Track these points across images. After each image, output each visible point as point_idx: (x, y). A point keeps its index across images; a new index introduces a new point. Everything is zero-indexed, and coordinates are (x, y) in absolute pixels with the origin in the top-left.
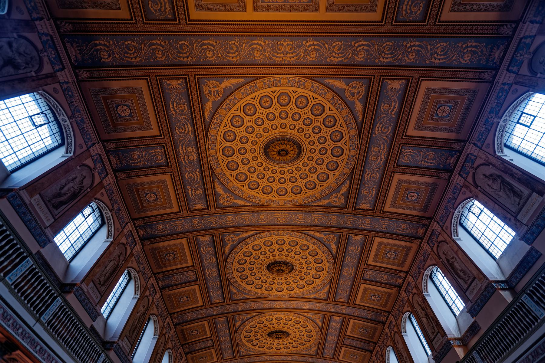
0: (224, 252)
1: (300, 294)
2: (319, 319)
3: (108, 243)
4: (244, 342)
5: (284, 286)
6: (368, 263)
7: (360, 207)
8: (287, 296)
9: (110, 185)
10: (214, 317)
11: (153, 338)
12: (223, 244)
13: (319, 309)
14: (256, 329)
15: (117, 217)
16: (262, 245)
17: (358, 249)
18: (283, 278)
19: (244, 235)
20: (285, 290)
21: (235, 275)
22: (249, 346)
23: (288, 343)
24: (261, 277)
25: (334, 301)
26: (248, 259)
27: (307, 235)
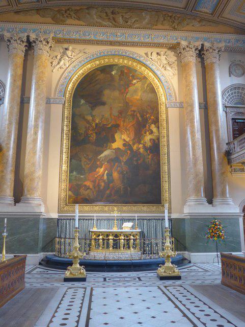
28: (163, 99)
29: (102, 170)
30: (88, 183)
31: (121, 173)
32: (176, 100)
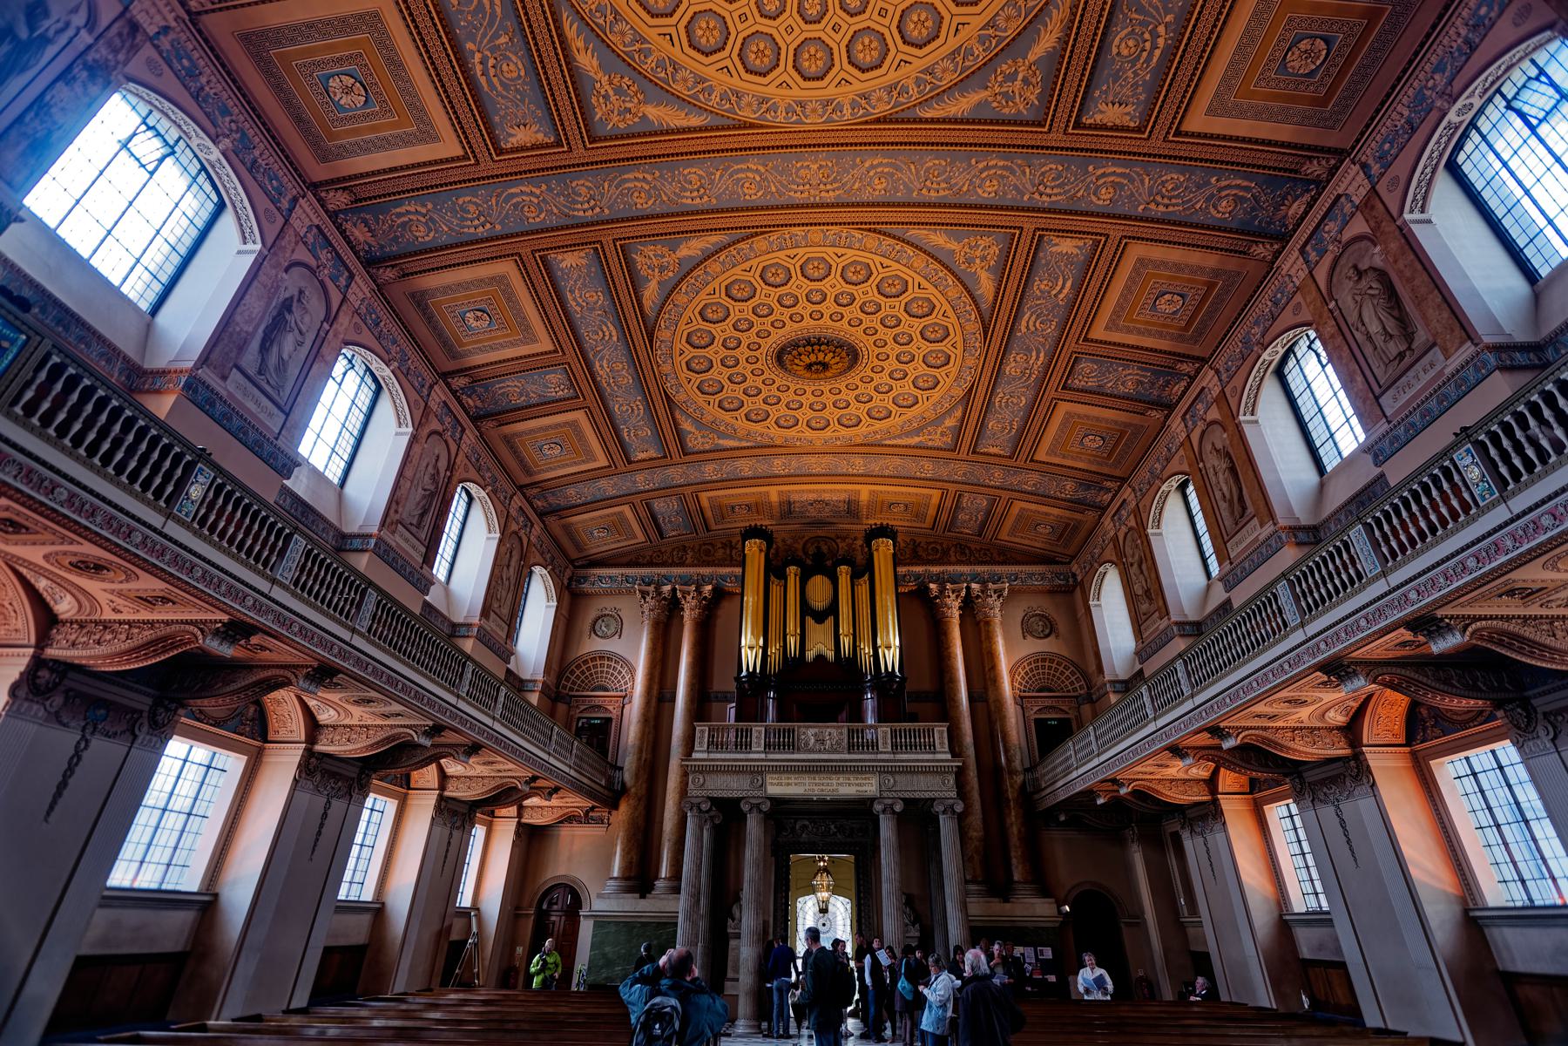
3: (250, 259)
5: (831, 414)
6: (1090, 336)
7: (1098, 117)
9: (172, 36)
10: (645, 496)
11: (488, 539)
12: (636, 283)
15: (250, 171)
16: (759, 284)
17: (1063, 287)
18: (826, 389)
19: (692, 248)
20: (834, 425)
24: (761, 386)
25: (974, 452)
26: (716, 329)
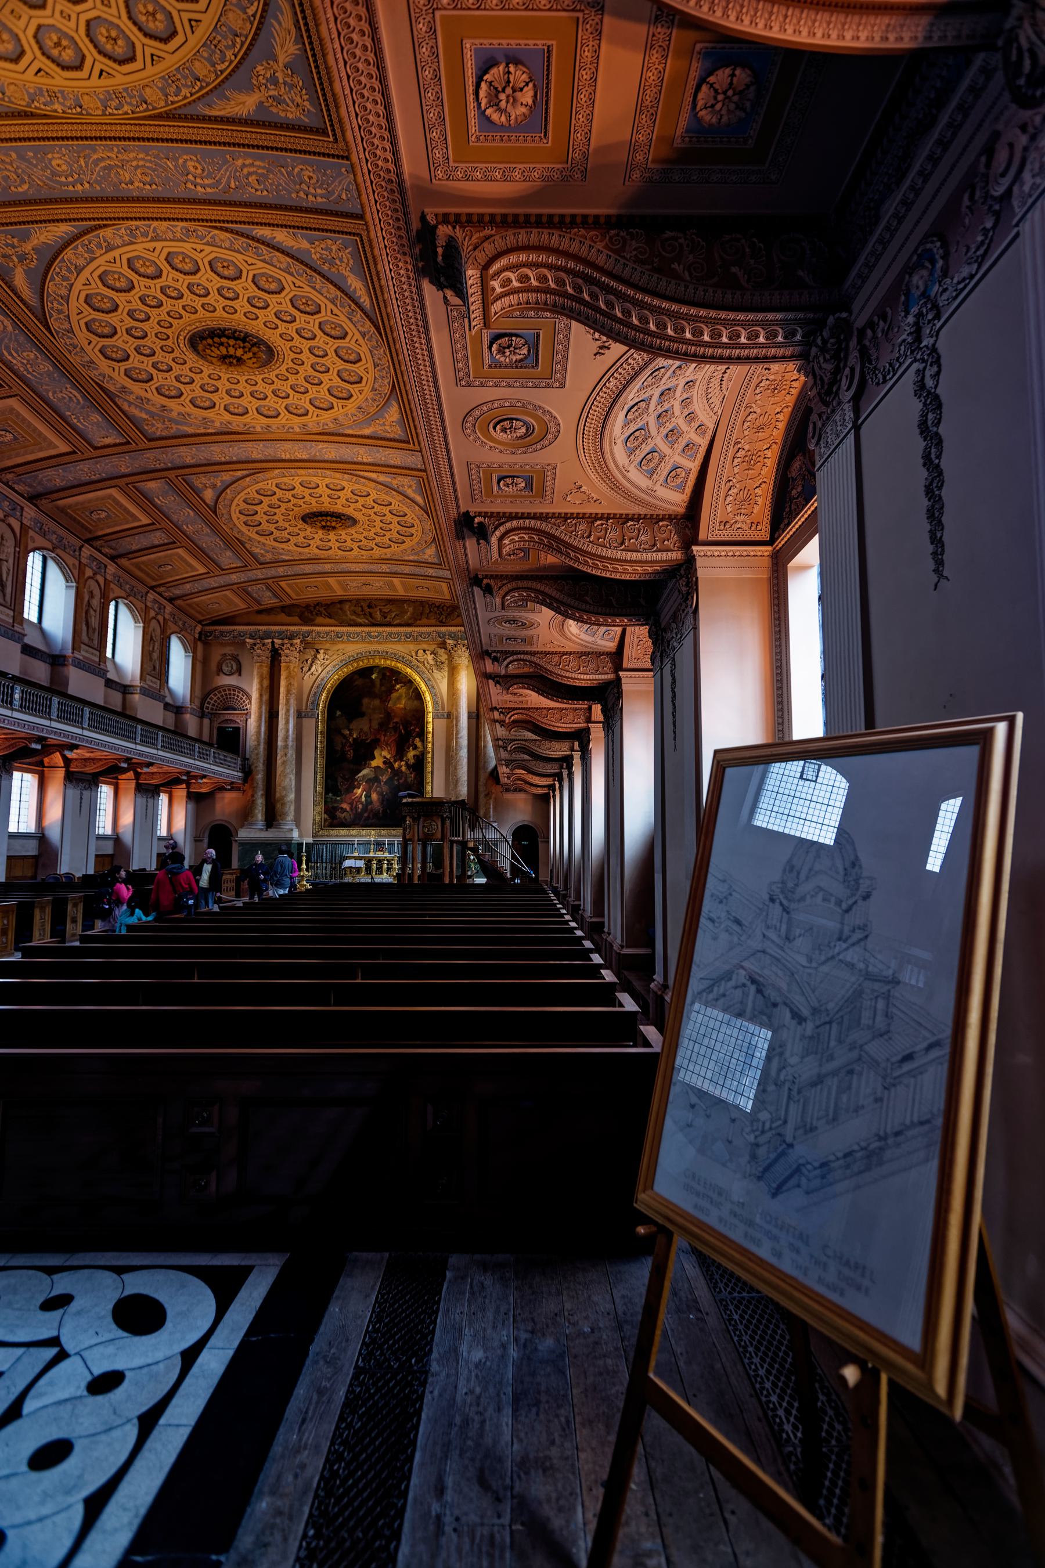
0: (22, 300)
1: (331, 425)
2: (410, 486)
4: (249, 534)
8: (297, 430)
13: (398, 463)
14: (265, 506)
21: (108, 371)
22: (268, 542)
23: (349, 540)
27: (253, 239)
28: (430, 707)
29: (360, 791)
30: (345, 806)
31: (380, 794)
32: (443, 709)
